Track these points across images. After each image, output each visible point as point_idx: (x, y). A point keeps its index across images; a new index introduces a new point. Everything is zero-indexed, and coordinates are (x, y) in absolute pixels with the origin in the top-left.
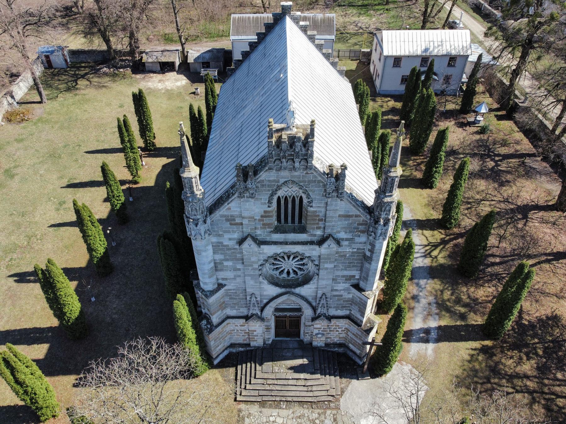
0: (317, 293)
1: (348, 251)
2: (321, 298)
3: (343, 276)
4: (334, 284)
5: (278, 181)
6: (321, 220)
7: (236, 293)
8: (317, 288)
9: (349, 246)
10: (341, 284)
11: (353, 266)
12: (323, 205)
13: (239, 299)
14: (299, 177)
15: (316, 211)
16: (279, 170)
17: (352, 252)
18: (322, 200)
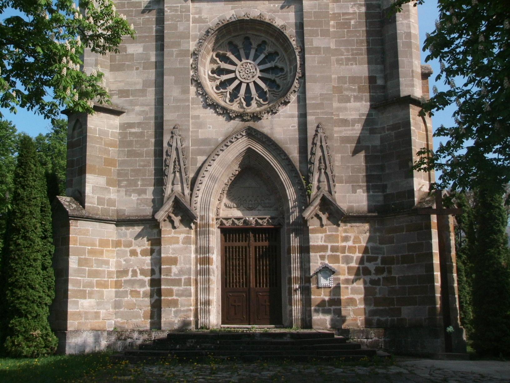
1: (351, 11)
7: (142, 134)
10: (353, 104)
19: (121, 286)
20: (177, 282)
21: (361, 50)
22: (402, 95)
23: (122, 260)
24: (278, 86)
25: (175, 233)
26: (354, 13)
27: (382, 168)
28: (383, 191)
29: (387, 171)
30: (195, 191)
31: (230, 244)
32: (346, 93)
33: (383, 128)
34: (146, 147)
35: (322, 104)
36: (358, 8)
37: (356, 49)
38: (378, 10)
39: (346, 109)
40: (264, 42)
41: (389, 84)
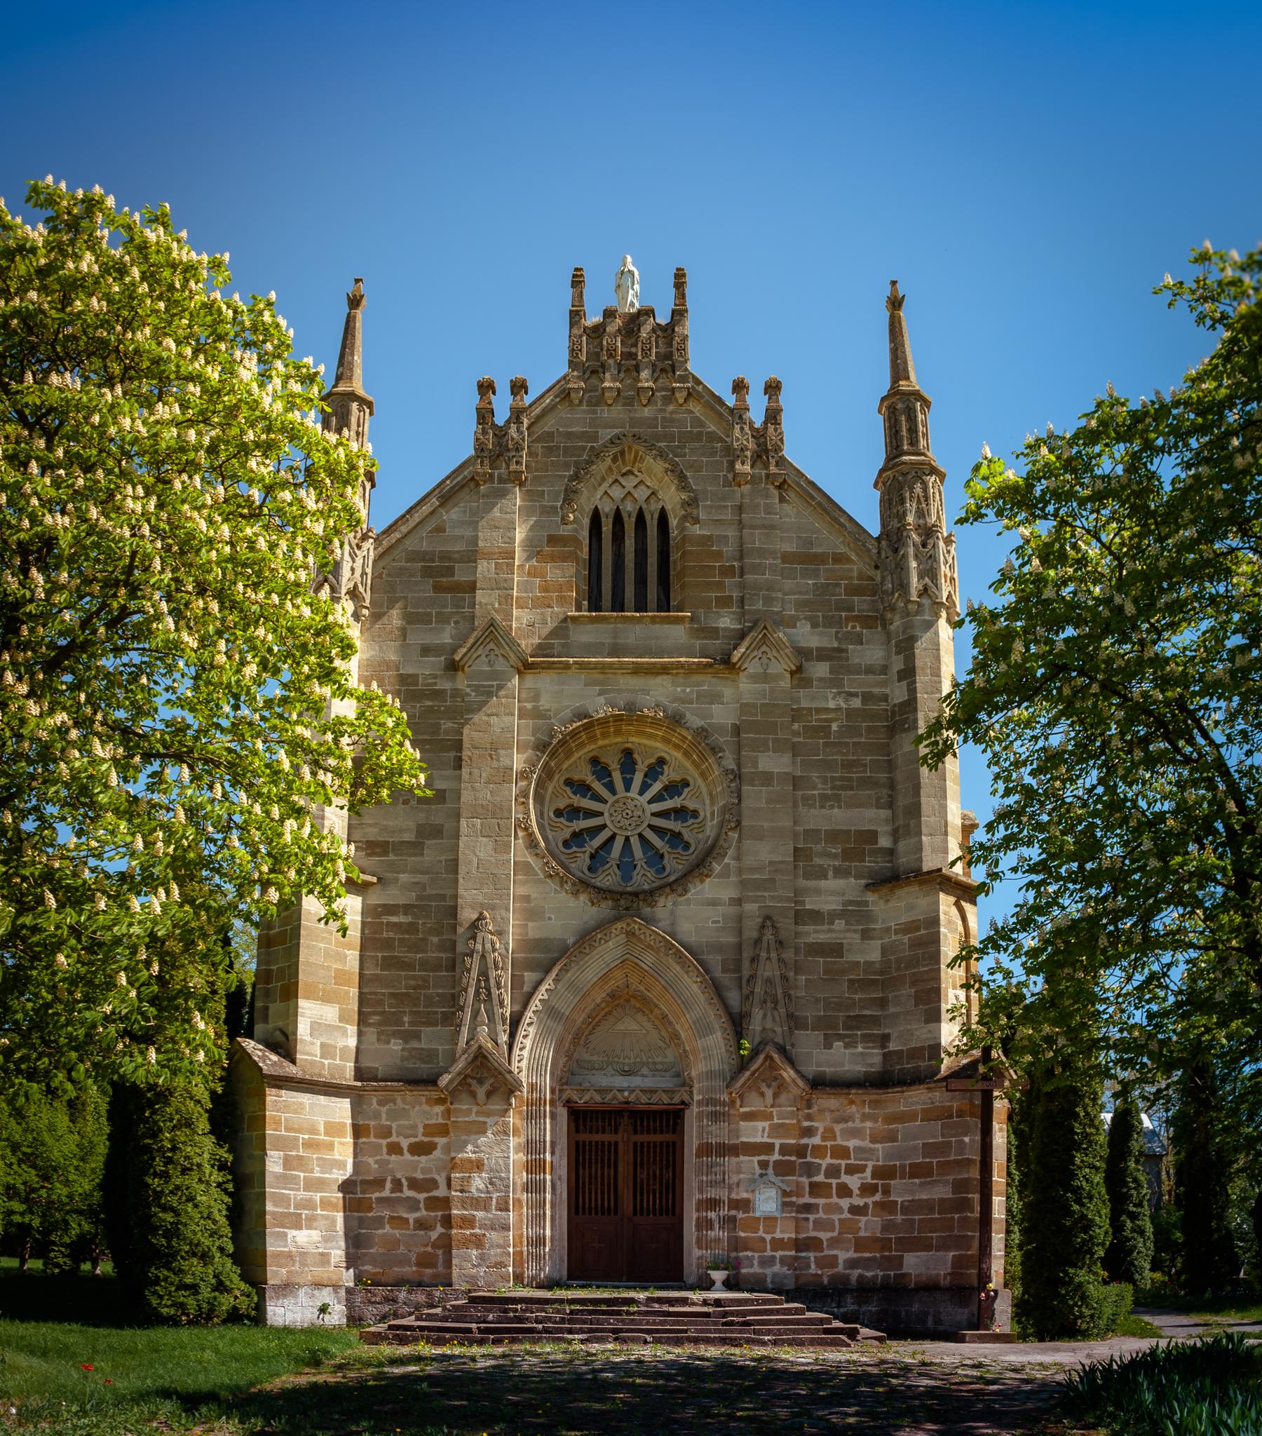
0: (740, 932)
1: (832, 705)
2: (757, 942)
3: (834, 836)
4: (802, 882)
5: (594, 437)
6: (728, 571)
8: (738, 902)
9: (834, 682)
10: (832, 883)
11: (864, 783)
12: (728, 516)
13: (424, 965)
14: (652, 423)
15: (710, 538)
16: (597, 404)
17: (851, 713)
18: (724, 499)
19: (370, 1209)
20: (483, 1204)
21: (850, 779)
22: (925, 869)
23: (371, 1160)
24: (687, 846)
25: (478, 1114)
26: (838, 709)
27: (883, 1003)
28: (883, 1047)
29: (892, 1010)
30: (519, 1038)
31: (584, 1137)
32: (818, 861)
33: (888, 929)
34: (423, 951)
35: (773, 881)
36: (846, 701)
37: (841, 779)
38: (883, 706)
39: (818, 891)
40: (661, 761)
41: (902, 846)
